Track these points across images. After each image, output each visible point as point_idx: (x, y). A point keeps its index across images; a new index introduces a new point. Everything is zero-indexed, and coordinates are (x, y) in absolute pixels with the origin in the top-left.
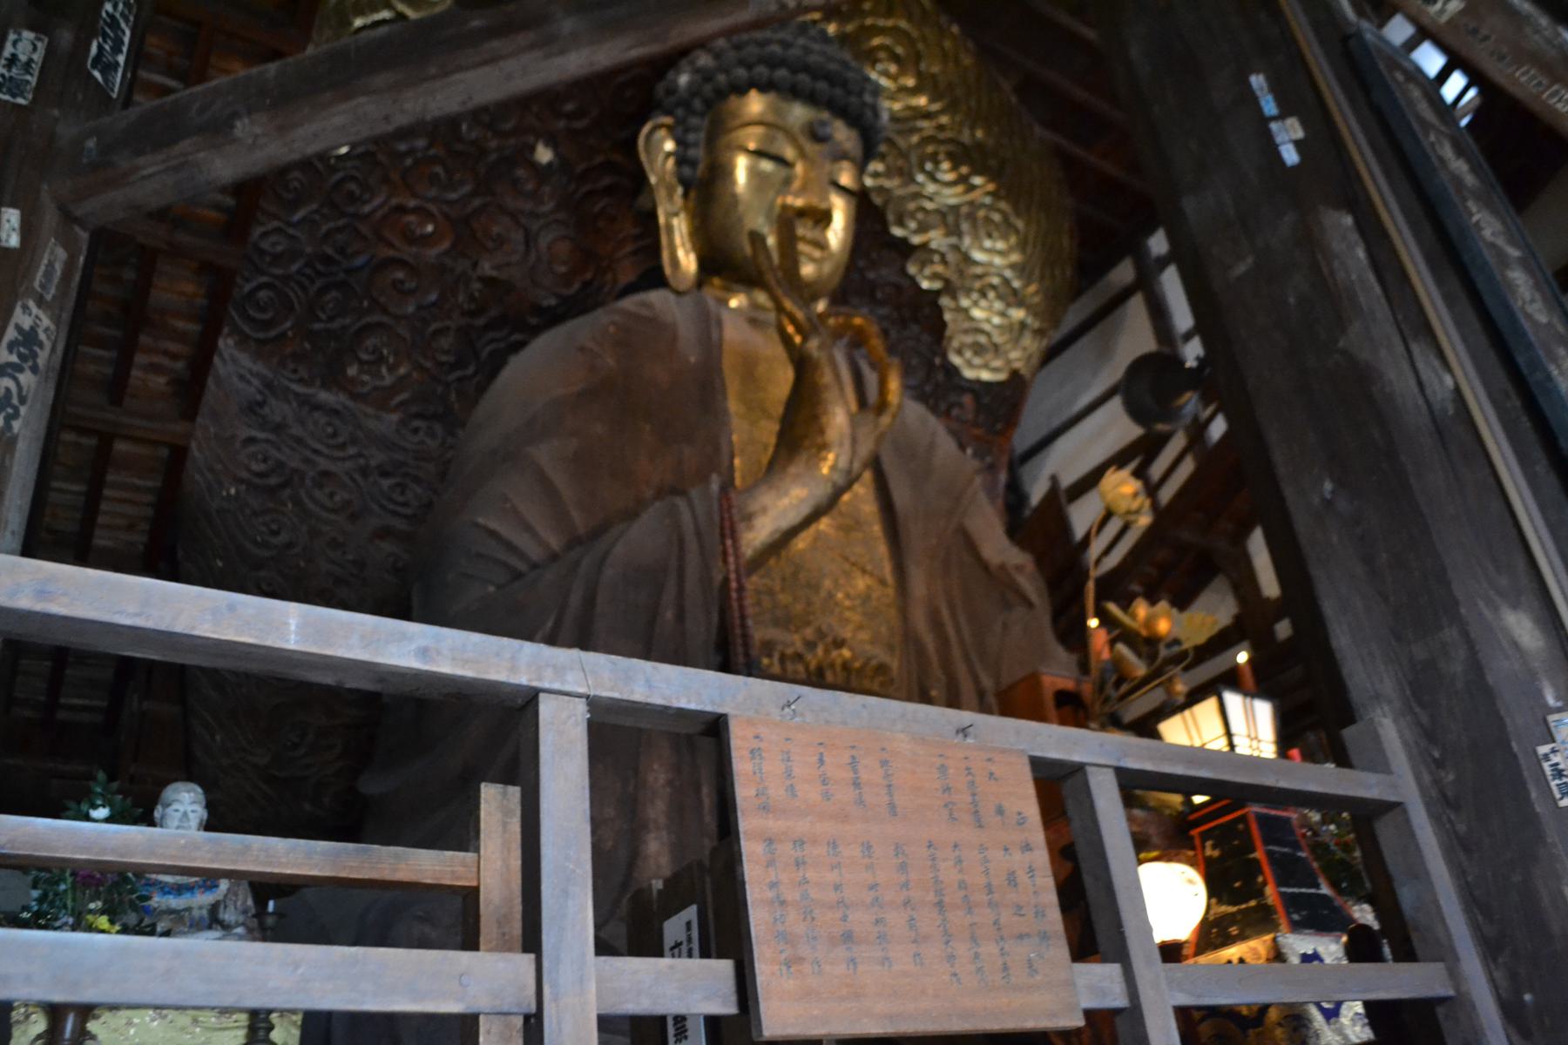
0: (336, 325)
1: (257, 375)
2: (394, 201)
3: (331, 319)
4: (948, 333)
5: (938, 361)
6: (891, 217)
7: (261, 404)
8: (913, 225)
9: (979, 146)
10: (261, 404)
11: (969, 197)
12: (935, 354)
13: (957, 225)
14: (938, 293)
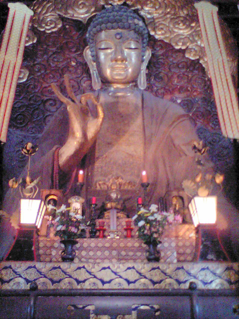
0: (39, 118)
1: (21, 135)
2: (44, 86)
3: (37, 117)
4: (206, 70)
5: (206, 79)
6: (173, 44)
7: (22, 142)
8: (181, 44)
9: (188, 15)
10: (22, 142)
11: (193, 30)
12: (205, 77)
13: (194, 39)
14: (198, 60)
